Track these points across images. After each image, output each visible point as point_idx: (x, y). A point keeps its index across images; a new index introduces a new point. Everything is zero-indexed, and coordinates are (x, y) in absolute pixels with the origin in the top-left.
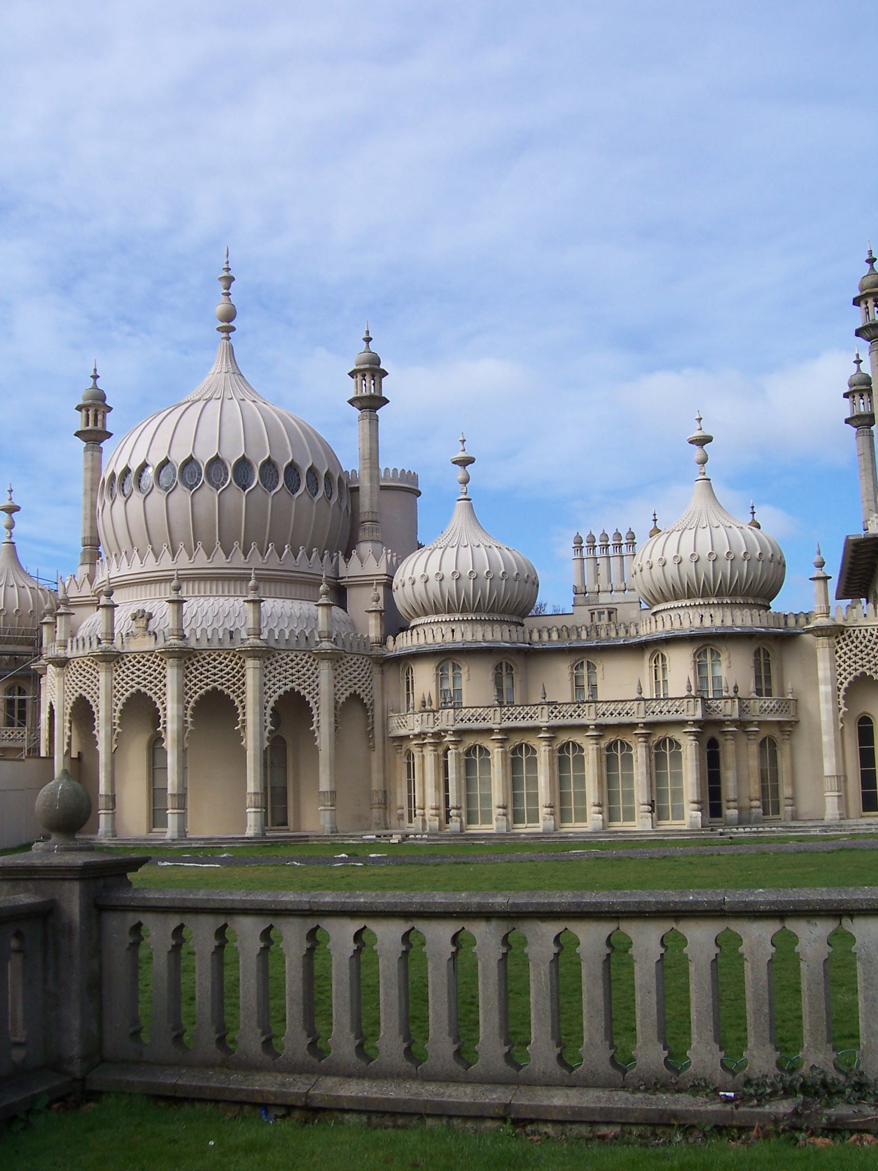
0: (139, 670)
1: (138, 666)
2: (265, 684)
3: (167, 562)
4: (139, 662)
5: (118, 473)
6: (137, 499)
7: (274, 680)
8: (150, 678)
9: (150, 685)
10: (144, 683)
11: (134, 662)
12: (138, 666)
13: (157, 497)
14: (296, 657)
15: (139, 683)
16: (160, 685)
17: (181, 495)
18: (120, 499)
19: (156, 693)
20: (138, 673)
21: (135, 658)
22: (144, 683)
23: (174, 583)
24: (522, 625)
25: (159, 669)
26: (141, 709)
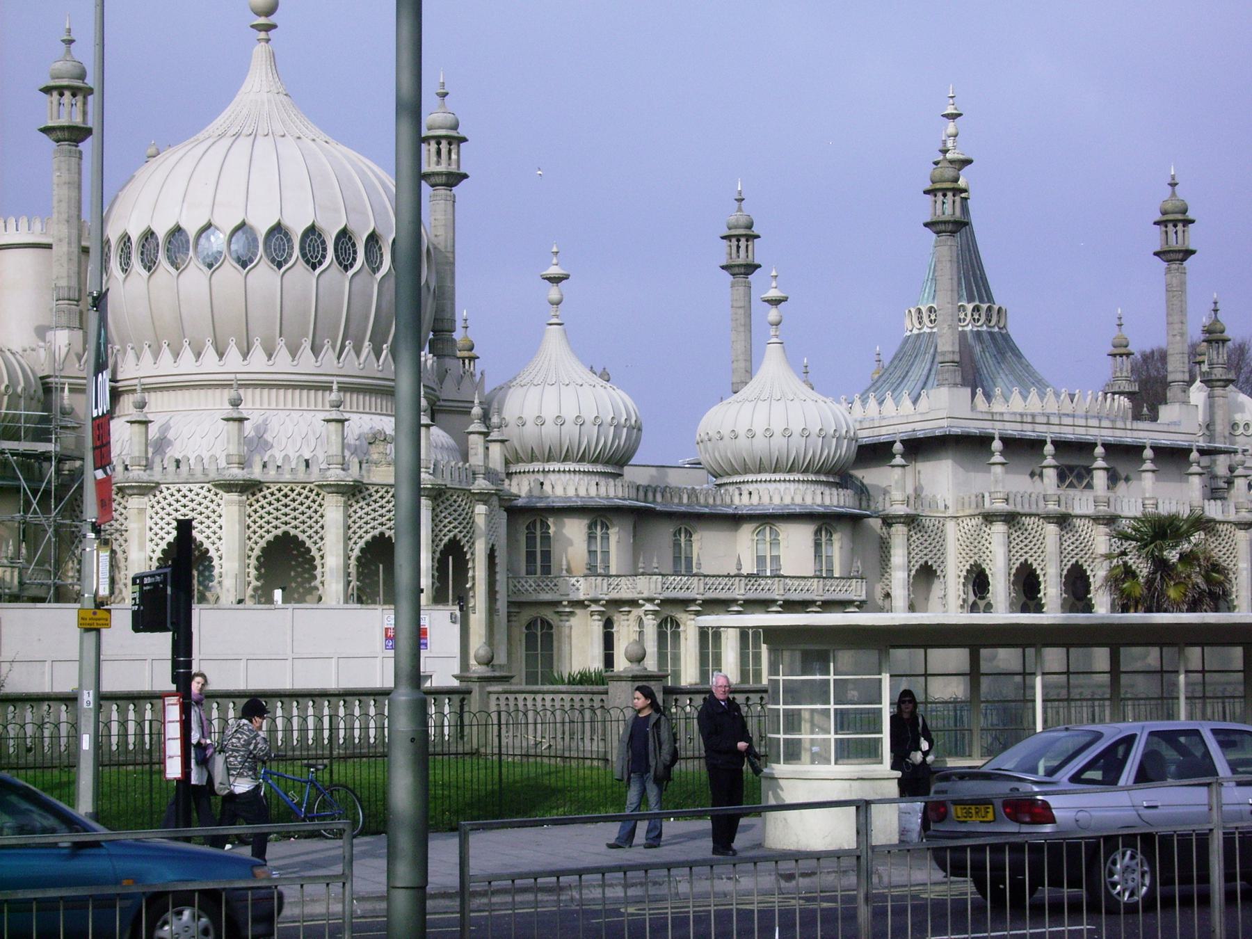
0: (286, 506)
1: (285, 501)
2: (349, 528)
4: (286, 496)
7: (361, 522)
8: (302, 518)
9: (302, 527)
10: (294, 523)
11: (279, 495)
12: (285, 501)
14: (292, 490)
15: (286, 523)
16: (317, 527)
19: (310, 537)
20: (284, 510)
21: (280, 490)
22: (294, 523)
23: (334, 396)
25: (315, 506)
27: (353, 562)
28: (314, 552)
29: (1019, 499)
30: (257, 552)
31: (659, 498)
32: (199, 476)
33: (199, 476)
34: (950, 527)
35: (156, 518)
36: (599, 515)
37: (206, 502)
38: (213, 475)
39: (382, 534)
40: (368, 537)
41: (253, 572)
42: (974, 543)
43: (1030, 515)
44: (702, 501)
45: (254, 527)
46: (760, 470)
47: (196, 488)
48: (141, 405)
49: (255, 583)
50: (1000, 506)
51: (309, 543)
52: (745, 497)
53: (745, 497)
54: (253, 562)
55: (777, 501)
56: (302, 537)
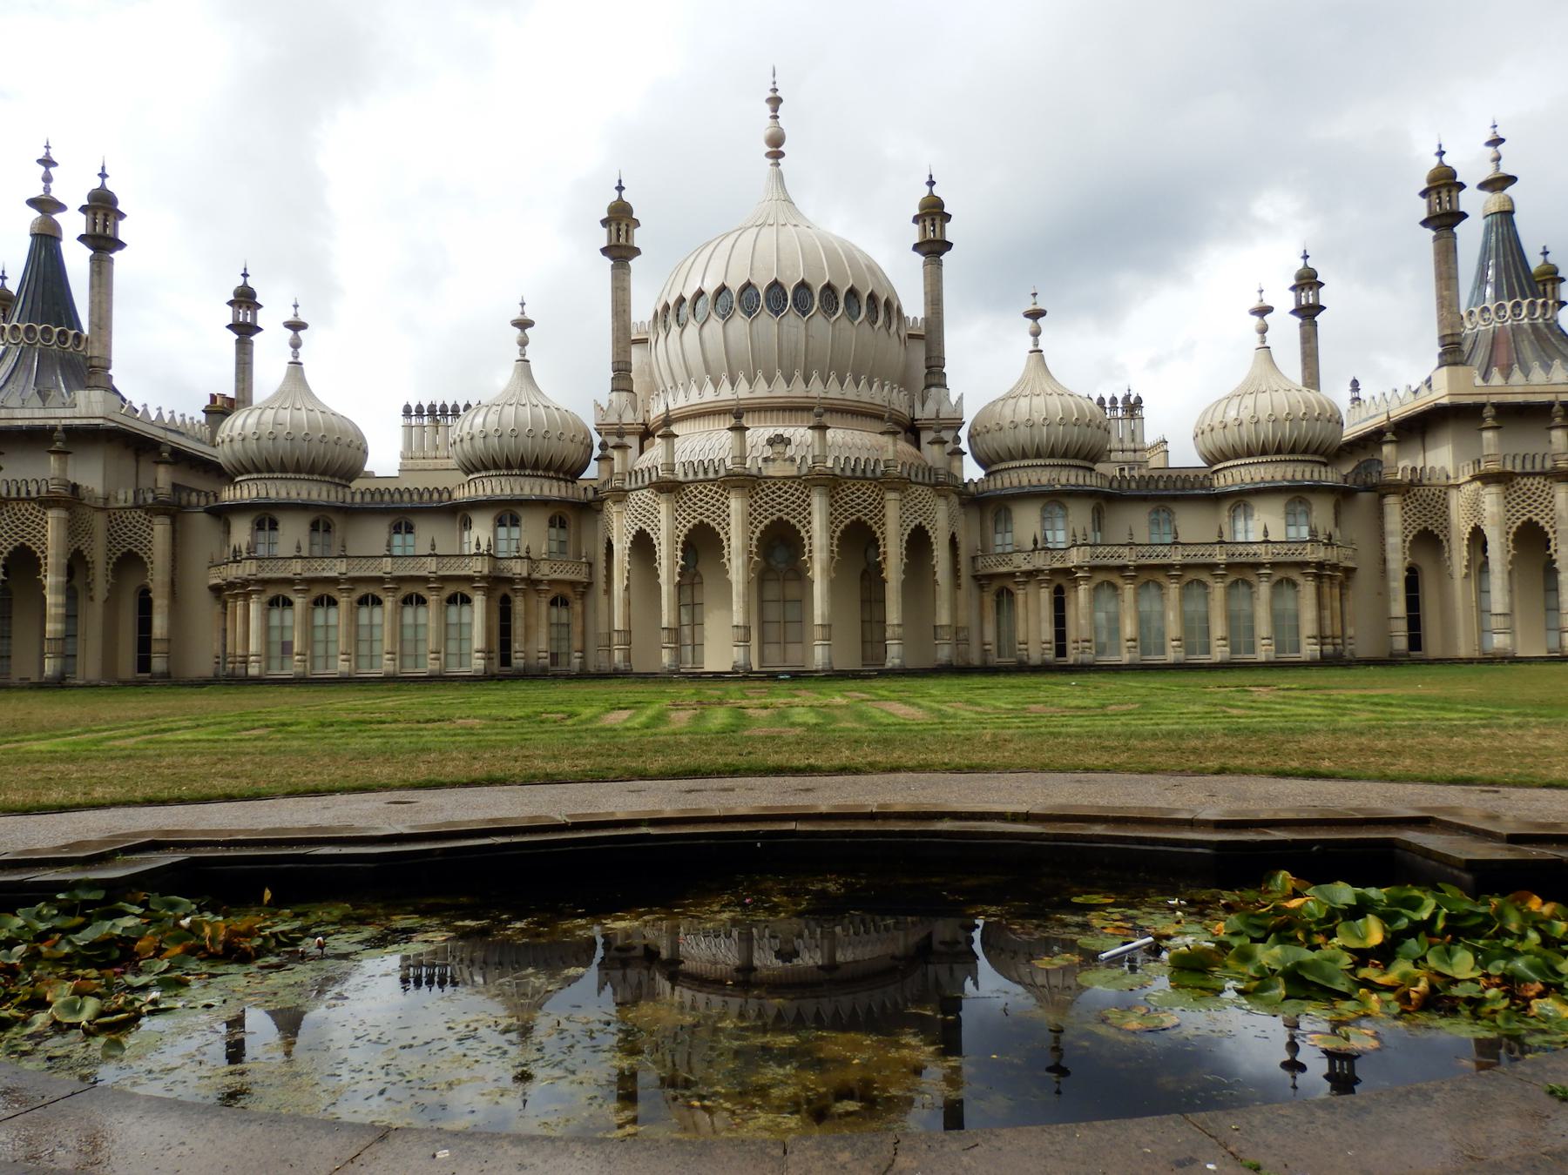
3: (726, 393)
5: (671, 304)
6: (692, 329)
13: (715, 324)
17: (739, 322)
18: (675, 329)
24: (1092, 470)
27: (754, 542)
28: (722, 535)
29: (1518, 462)
30: (682, 537)
31: (1133, 485)
34: (1453, 493)
36: (1053, 499)
38: (654, 479)
39: (780, 519)
40: (766, 522)
41: (680, 554)
42: (1475, 506)
43: (1534, 474)
44: (1179, 484)
50: (1493, 467)
54: (680, 546)
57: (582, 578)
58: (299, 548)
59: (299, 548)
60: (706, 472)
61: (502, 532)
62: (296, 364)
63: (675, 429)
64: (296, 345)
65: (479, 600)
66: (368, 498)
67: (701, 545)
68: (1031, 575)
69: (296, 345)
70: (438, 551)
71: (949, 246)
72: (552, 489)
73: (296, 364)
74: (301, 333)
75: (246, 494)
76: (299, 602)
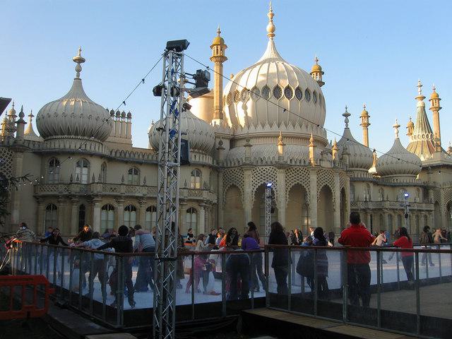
26: (298, 191)
30: (289, 189)
32: (269, 163)
33: (269, 163)
34: (442, 192)
35: (254, 178)
37: (272, 173)
41: (288, 196)
45: (288, 181)
46: (400, 173)
47: (268, 167)
48: (248, 141)
49: (288, 200)
51: (305, 187)
52: (395, 181)
53: (395, 181)
55: (405, 181)
56: (303, 185)
57: (215, 201)
58: (123, 179)
59: (123, 179)
60: (300, 162)
61: (193, 178)
62: (78, 80)
63: (252, 142)
64: (79, 70)
65: (202, 212)
66: (118, 155)
67: (298, 191)
68: (364, 210)
69: (79, 70)
70: (187, 187)
71: (324, 83)
72: (208, 160)
73: (78, 80)
74: (82, 64)
75: (53, 146)
76: (121, 208)
